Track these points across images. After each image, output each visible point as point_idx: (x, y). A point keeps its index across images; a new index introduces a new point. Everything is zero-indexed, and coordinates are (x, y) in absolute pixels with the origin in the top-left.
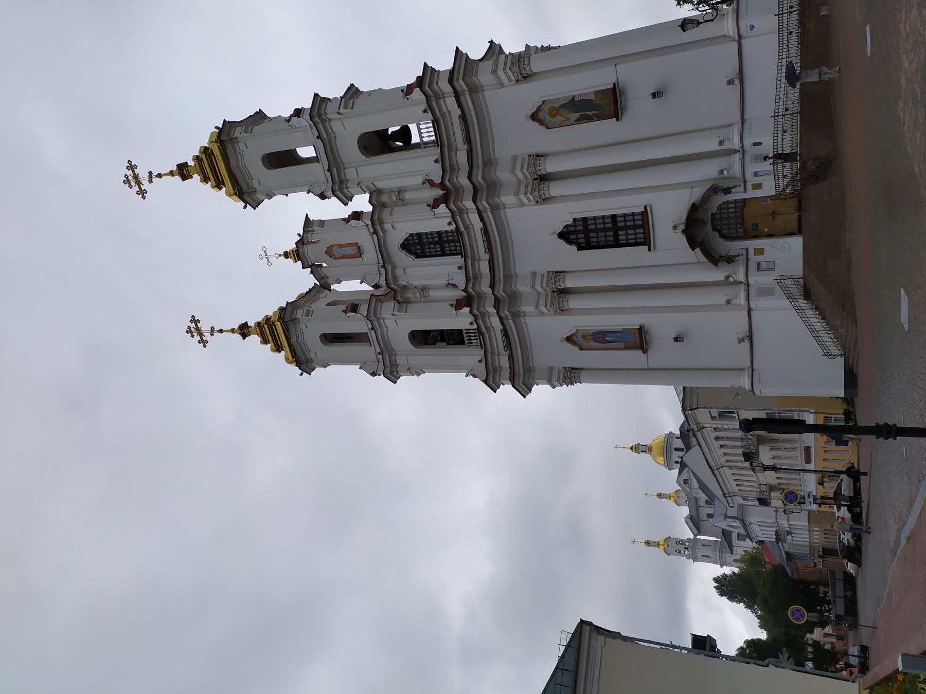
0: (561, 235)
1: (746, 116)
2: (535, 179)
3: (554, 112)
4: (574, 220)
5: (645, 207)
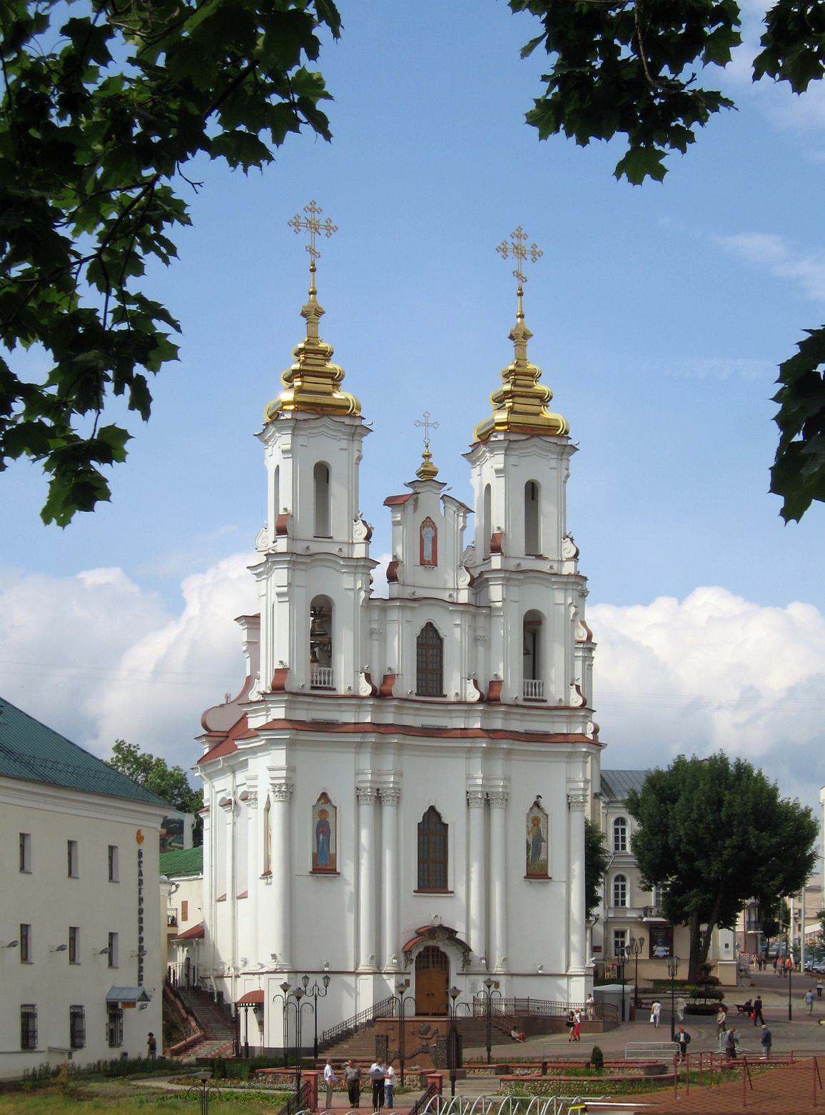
0: (432, 808)
1: (515, 978)
2: (487, 794)
3: (536, 822)
4: (446, 826)
5: (452, 892)
